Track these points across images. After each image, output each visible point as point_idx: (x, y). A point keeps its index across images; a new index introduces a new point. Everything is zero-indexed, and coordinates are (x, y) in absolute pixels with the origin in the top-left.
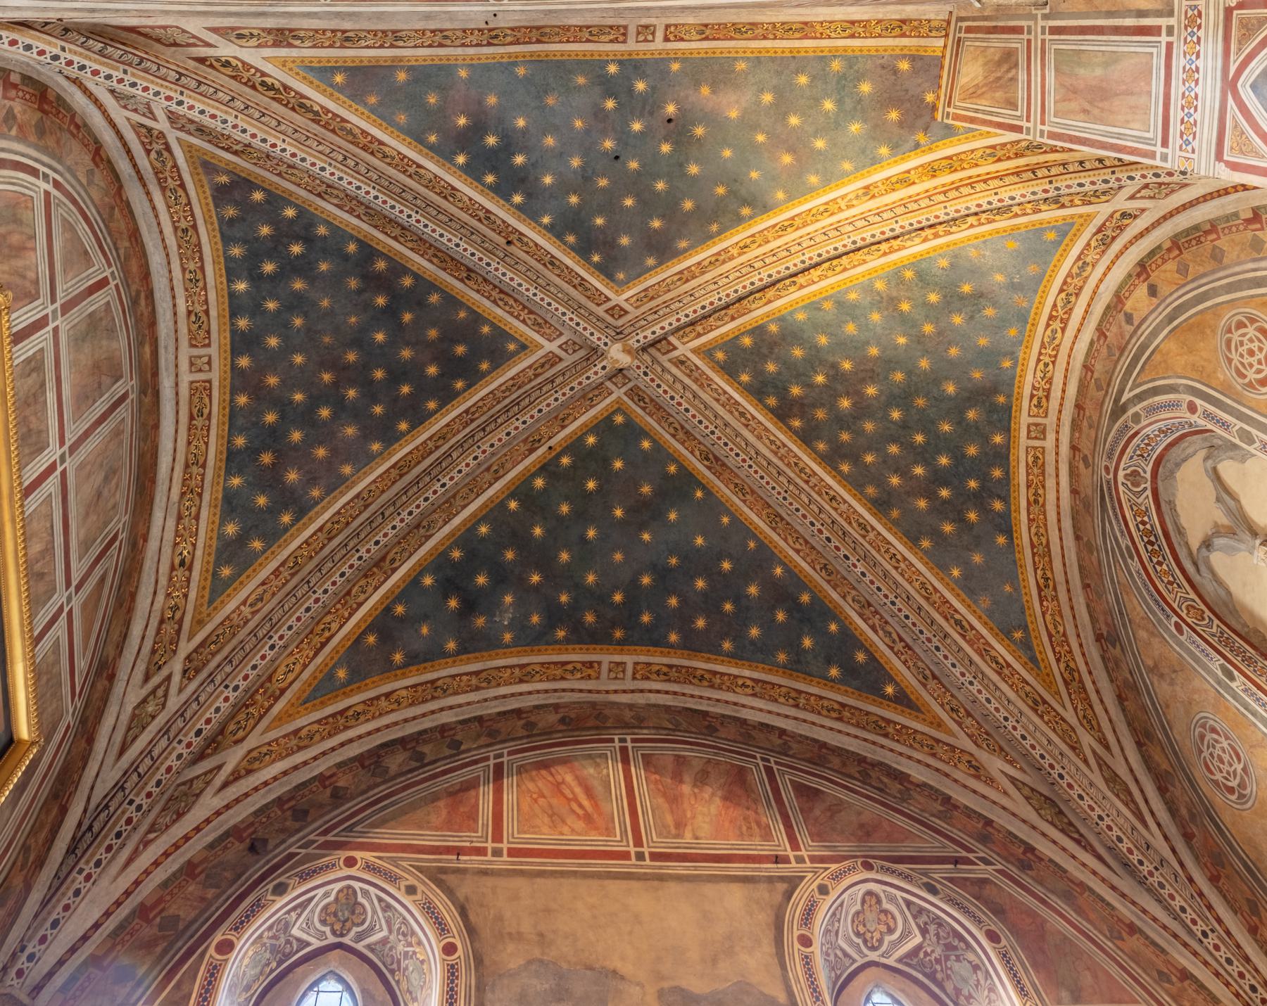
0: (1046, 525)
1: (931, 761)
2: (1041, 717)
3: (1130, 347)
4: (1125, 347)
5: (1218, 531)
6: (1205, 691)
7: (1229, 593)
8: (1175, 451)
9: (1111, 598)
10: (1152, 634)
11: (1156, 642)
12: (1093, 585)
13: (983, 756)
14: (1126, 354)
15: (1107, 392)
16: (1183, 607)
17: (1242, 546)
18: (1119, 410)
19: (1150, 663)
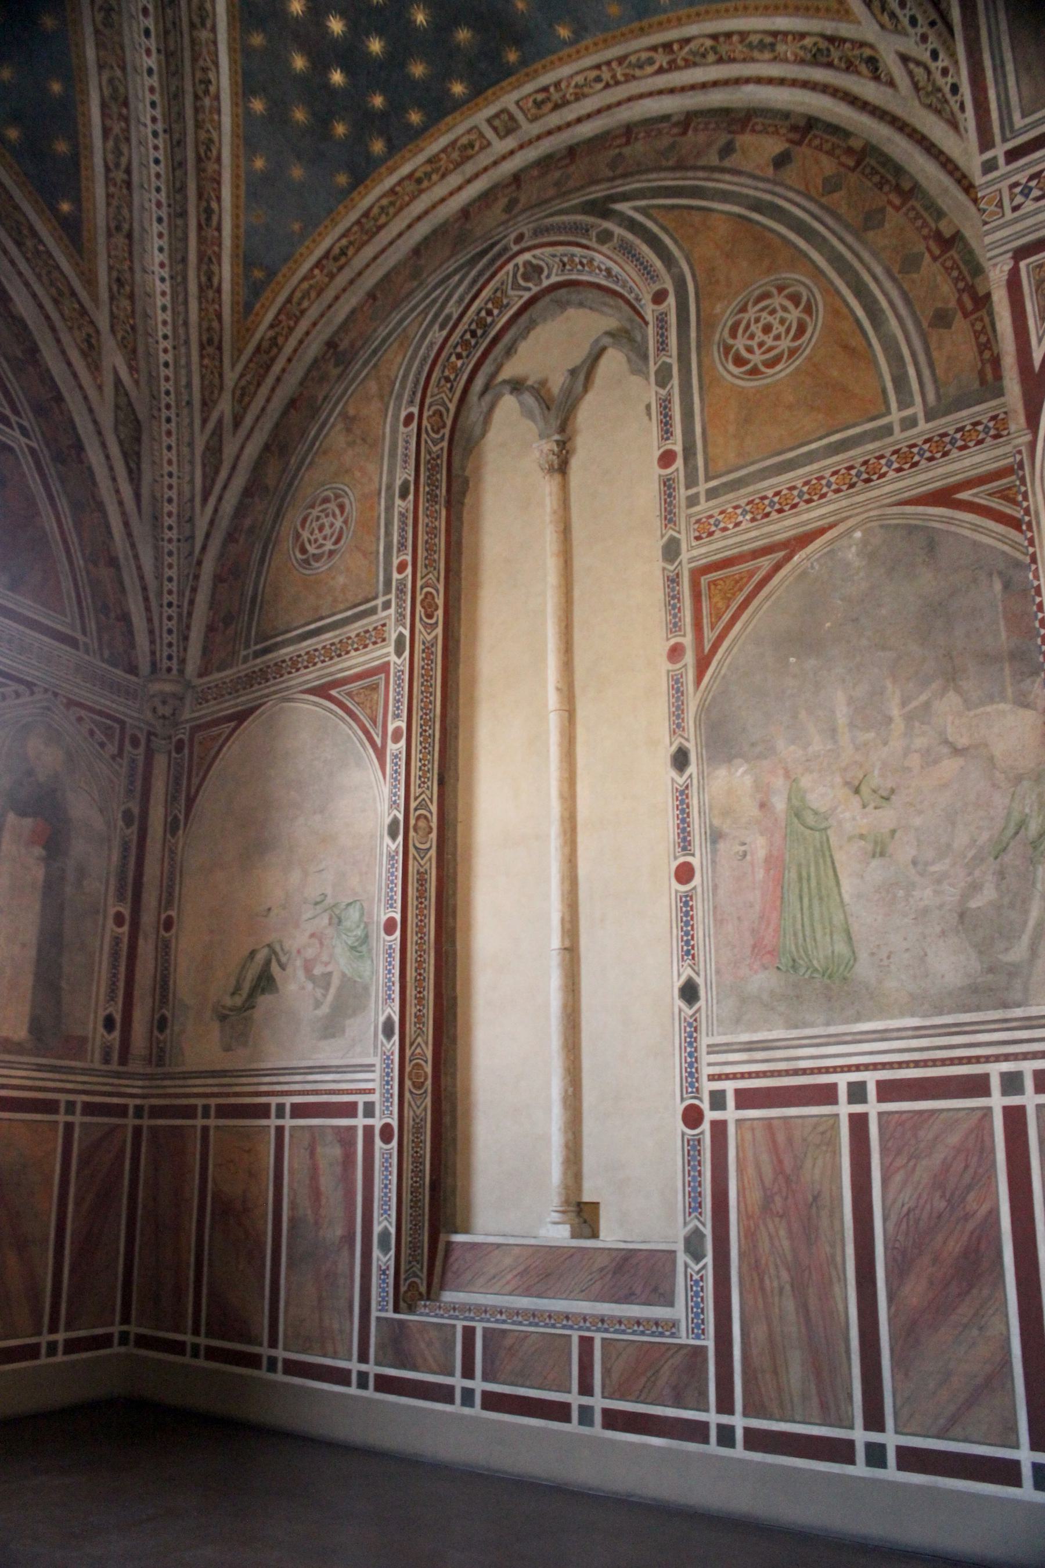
0: (401, 209)
1: (49, 306)
2: (202, 357)
3: (690, 174)
4: (686, 169)
5: (540, 392)
6: (371, 480)
7: (483, 434)
8: (592, 295)
9: (383, 332)
10: (381, 397)
11: (376, 405)
12: (379, 303)
13: (109, 344)
14: (678, 175)
15: (612, 179)
16: (433, 408)
17: (541, 424)
18: (601, 209)
19: (351, 412)
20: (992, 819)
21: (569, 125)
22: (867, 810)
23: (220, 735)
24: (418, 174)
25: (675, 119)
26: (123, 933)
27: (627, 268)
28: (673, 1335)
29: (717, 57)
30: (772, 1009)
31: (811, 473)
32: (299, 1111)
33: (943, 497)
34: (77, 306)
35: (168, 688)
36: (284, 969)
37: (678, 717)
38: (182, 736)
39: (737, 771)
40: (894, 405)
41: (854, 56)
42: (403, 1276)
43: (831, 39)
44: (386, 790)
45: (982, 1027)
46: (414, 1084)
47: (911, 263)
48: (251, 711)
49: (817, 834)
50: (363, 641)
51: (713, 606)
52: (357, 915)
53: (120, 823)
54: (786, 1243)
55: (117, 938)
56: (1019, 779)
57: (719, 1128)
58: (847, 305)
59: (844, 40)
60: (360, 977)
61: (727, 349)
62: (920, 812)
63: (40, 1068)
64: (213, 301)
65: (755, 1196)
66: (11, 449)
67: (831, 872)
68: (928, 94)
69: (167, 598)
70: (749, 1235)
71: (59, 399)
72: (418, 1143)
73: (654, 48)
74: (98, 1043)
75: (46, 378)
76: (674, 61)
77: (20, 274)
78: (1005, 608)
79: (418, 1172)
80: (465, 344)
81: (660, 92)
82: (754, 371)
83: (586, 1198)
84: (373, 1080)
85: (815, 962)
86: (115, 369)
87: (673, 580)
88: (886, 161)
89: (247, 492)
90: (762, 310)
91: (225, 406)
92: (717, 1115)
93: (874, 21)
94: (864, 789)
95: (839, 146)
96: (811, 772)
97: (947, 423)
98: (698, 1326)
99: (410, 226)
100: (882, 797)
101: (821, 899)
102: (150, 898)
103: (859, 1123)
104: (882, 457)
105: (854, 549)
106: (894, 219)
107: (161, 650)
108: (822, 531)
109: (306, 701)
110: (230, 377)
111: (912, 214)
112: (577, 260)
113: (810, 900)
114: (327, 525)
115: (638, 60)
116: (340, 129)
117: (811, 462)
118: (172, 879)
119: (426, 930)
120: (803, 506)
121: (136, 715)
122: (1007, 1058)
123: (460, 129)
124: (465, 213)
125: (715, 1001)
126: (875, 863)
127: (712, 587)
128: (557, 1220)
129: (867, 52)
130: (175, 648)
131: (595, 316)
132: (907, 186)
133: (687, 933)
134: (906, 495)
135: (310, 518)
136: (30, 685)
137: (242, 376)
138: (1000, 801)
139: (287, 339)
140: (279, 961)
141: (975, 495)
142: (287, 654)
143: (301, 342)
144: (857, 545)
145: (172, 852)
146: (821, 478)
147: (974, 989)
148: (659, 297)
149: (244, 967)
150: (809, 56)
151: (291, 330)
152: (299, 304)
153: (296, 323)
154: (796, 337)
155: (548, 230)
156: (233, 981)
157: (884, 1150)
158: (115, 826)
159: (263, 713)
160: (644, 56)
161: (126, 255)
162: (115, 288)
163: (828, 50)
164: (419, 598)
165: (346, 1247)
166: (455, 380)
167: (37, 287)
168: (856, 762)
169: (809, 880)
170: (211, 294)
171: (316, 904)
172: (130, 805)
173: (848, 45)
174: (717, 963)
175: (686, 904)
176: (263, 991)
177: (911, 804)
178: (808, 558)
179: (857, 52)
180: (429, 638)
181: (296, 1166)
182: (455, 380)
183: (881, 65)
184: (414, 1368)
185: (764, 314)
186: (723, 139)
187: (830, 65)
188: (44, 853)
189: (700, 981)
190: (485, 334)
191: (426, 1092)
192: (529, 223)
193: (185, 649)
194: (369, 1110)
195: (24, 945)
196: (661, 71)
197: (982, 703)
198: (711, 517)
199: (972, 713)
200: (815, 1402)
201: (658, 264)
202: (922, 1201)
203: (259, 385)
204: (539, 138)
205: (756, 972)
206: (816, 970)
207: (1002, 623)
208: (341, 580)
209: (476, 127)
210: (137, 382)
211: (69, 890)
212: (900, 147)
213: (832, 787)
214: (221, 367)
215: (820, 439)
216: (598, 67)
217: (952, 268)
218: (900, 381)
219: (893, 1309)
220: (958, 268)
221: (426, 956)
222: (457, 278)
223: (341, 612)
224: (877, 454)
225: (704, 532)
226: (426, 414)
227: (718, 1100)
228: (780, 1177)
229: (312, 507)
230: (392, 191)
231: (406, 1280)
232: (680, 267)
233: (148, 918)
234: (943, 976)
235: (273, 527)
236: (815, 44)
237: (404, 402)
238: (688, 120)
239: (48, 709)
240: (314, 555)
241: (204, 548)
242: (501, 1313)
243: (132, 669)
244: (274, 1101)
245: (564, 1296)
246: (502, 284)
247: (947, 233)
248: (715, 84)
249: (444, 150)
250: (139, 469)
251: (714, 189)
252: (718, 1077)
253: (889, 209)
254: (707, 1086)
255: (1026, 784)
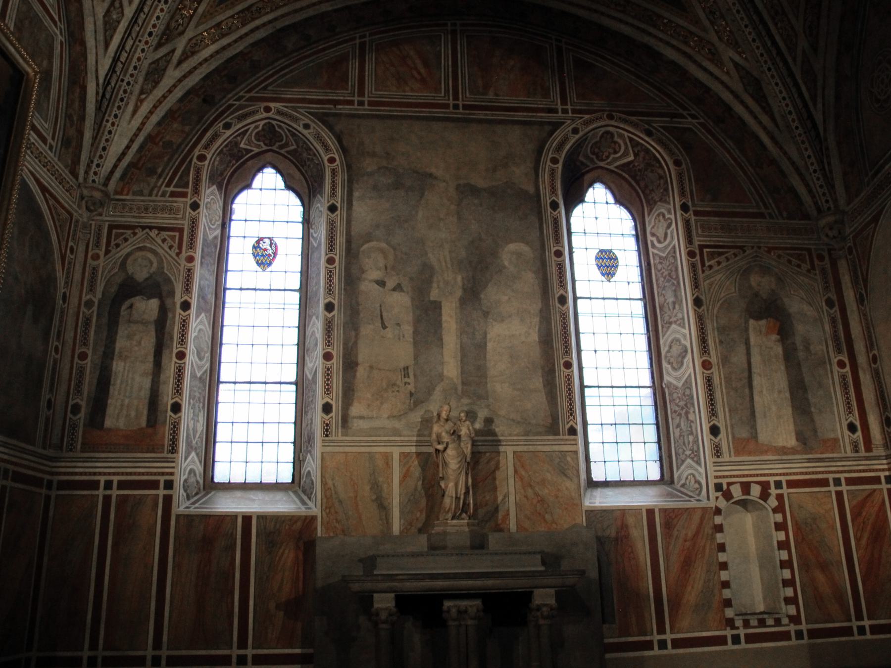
2: (776, 25)
26: (847, 372)
34: (696, 39)
35: (831, 219)
38: (849, 244)
48: (881, 212)
53: (825, 308)
55: (844, 375)
63: (809, 460)
66: (690, 129)
69: (811, 169)
71: (708, 90)
74: (847, 441)
75: (697, 82)
77: (661, 40)
86: (731, 59)
102: (860, 347)
107: (820, 199)
118: (869, 332)
121: (817, 242)
130: (828, 195)
136: (742, 248)
145: (865, 315)
158: (823, 311)
162: (711, 18)
167: (674, 42)
172: (830, 295)
188: (778, 337)
193: (835, 193)
195: (780, 392)
210: (746, 59)
211: (801, 355)
233: (862, 359)
239: (757, 256)
241: (825, 130)
243: (806, 216)
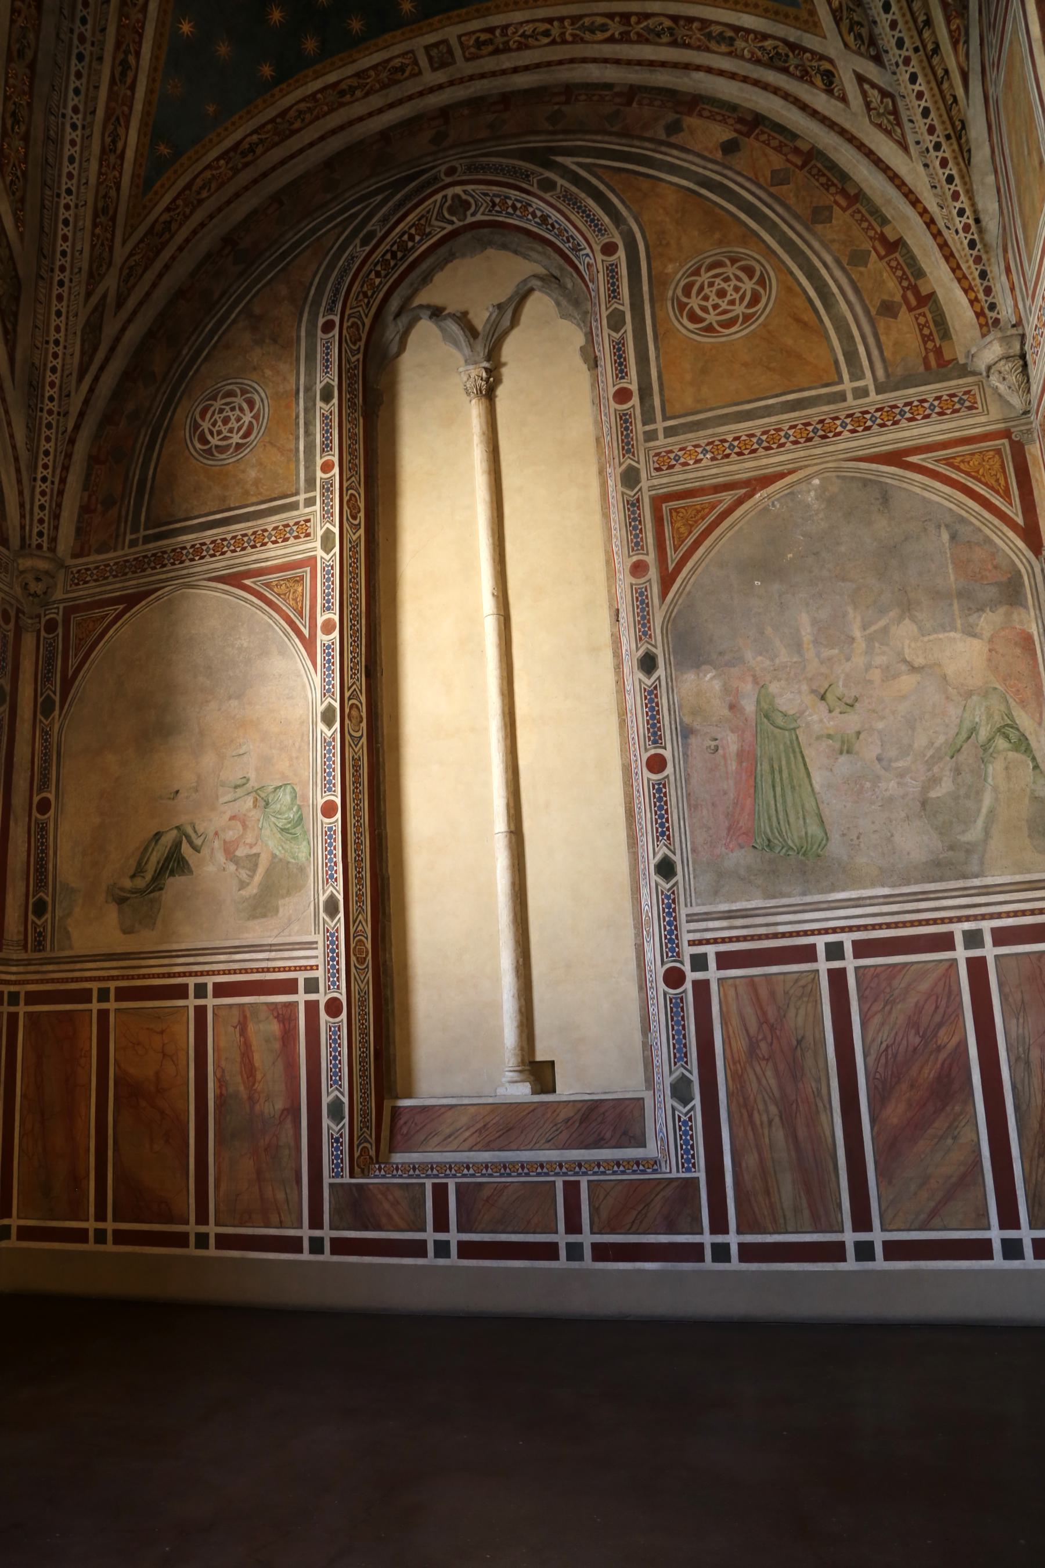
0: (317, 118)
3: (636, 143)
7: (399, 354)
14: (624, 141)
17: (467, 351)
18: (544, 158)
19: (257, 311)
20: (947, 726)
21: (504, 72)
22: (833, 714)
23: (104, 617)
24: (343, 86)
25: (617, 89)
27: (573, 217)
28: (655, 1171)
29: (672, 39)
30: (750, 882)
31: (770, 424)
32: (221, 990)
33: (895, 458)
35: (43, 565)
36: (199, 852)
37: (644, 626)
39: (705, 676)
40: (846, 376)
41: (811, 67)
42: (356, 1143)
43: (793, 46)
44: (317, 679)
45: (946, 894)
46: (357, 958)
47: (858, 258)
49: (787, 733)
50: (283, 535)
51: (675, 531)
52: (288, 798)
54: (773, 1082)
56: (969, 694)
57: (702, 988)
58: (800, 284)
59: (805, 50)
60: (294, 858)
61: (682, 306)
62: (882, 718)
64: (114, 168)
65: (741, 1044)
67: (801, 766)
68: (879, 115)
70: (736, 1077)
72: (363, 1016)
73: (611, 16)
76: (628, 33)
78: (952, 554)
79: (364, 1043)
80: (385, 263)
81: (606, 61)
82: (709, 329)
83: (540, 1057)
84: (318, 956)
85: (790, 843)
87: (633, 505)
88: (833, 166)
89: (126, 376)
90: (716, 276)
91: (110, 283)
92: (699, 975)
93: (839, 38)
94: (829, 696)
95: (786, 145)
96: (779, 680)
97: (897, 397)
98: (688, 1161)
99: (322, 138)
100: (847, 704)
101: (793, 788)
103: (837, 978)
104: (837, 418)
105: (812, 494)
106: (840, 217)
107: (31, 525)
108: (782, 476)
109: (216, 590)
110: (120, 254)
111: (858, 216)
112: (510, 202)
113: (782, 789)
114: (233, 418)
115: (593, 23)
116: (276, 15)
117: (769, 415)
119: (361, 813)
120: (761, 452)
122: (968, 918)
123: (397, 50)
124: (385, 136)
125: (692, 876)
126: (843, 759)
127: (674, 514)
128: (515, 1079)
129: (826, 66)
130: (46, 525)
131: (519, 259)
132: (852, 192)
133: (661, 817)
134: (861, 453)
135: (212, 409)
137: (131, 255)
138: (954, 712)
139: (181, 226)
140: (191, 843)
141: (924, 460)
142: (187, 541)
143: (195, 232)
144: (816, 491)
146: (780, 430)
147: (938, 864)
148: (609, 249)
149: (146, 849)
150: (766, 58)
151: (187, 217)
152: (199, 193)
153: (192, 213)
154: (750, 305)
155: (485, 168)
156: (133, 863)
157: (861, 998)
159: (158, 598)
160: (600, 20)
161: (26, 89)
162: (9, 122)
163: (787, 56)
164: (346, 499)
165: (290, 1118)
166: (372, 296)
168: (822, 674)
169: (780, 772)
170: (112, 158)
171: (236, 787)
173: (808, 55)
174: (692, 843)
175: (659, 791)
176: (172, 873)
177: (874, 711)
178: (769, 497)
179: (814, 64)
180: (354, 538)
181: (222, 1044)
182: (372, 296)
183: (836, 81)
184: (379, 1228)
185: (718, 280)
186: (671, 116)
187: (785, 71)
189: (677, 859)
190: (404, 258)
191: (367, 967)
192: (461, 158)
193: (56, 528)
194: (312, 986)
196: (611, 40)
197: (935, 631)
198: (671, 452)
199: (926, 639)
200: (806, 1213)
201: (606, 220)
202: (898, 1039)
203: (146, 269)
204: (472, 78)
205: (732, 851)
206: (791, 848)
207: (950, 567)
208: (253, 473)
209: (412, 52)
210: (21, 236)
212: (846, 157)
213: (800, 692)
214: (112, 240)
215: (777, 396)
216: (550, 21)
217: (896, 268)
218: (851, 356)
219: (876, 1129)
220: (902, 269)
221: (363, 838)
222: (380, 198)
223: (253, 504)
224: (832, 416)
225: (664, 463)
226: (345, 325)
227: (699, 962)
228: (765, 1026)
229: (214, 398)
230: (313, 96)
231: (358, 1146)
232: (629, 225)
234: (909, 854)
235: (163, 415)
236: (775, 48)
237: (322, 309)
238: (632, 93)
240: (217, 447)
242: (468, 1168)
244: (192, 982)
245: (529, 1147)
246: (428, 212)
247: (892, 237)
248: (663, 64)
249: (374, 67)
250: (15, 331)
251: (662, 160)
252: (700, 942)
253: (836, 209)
254: (688, 951)
255: (975, 698)
